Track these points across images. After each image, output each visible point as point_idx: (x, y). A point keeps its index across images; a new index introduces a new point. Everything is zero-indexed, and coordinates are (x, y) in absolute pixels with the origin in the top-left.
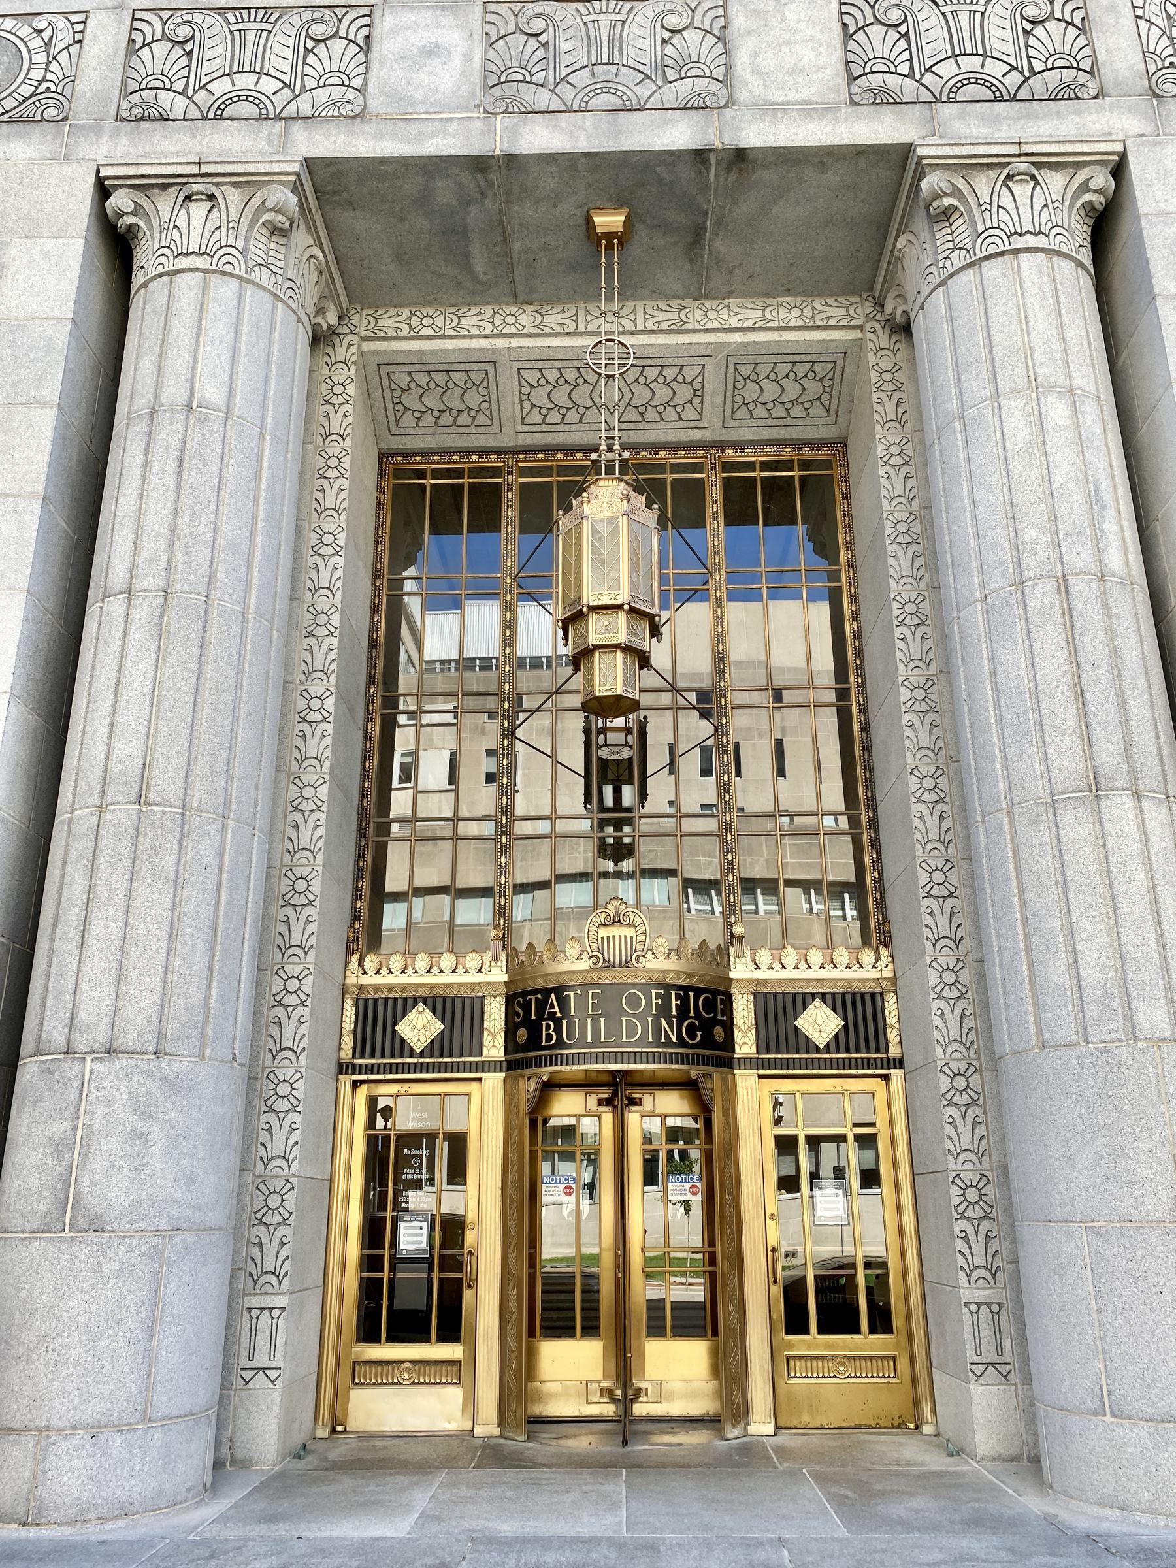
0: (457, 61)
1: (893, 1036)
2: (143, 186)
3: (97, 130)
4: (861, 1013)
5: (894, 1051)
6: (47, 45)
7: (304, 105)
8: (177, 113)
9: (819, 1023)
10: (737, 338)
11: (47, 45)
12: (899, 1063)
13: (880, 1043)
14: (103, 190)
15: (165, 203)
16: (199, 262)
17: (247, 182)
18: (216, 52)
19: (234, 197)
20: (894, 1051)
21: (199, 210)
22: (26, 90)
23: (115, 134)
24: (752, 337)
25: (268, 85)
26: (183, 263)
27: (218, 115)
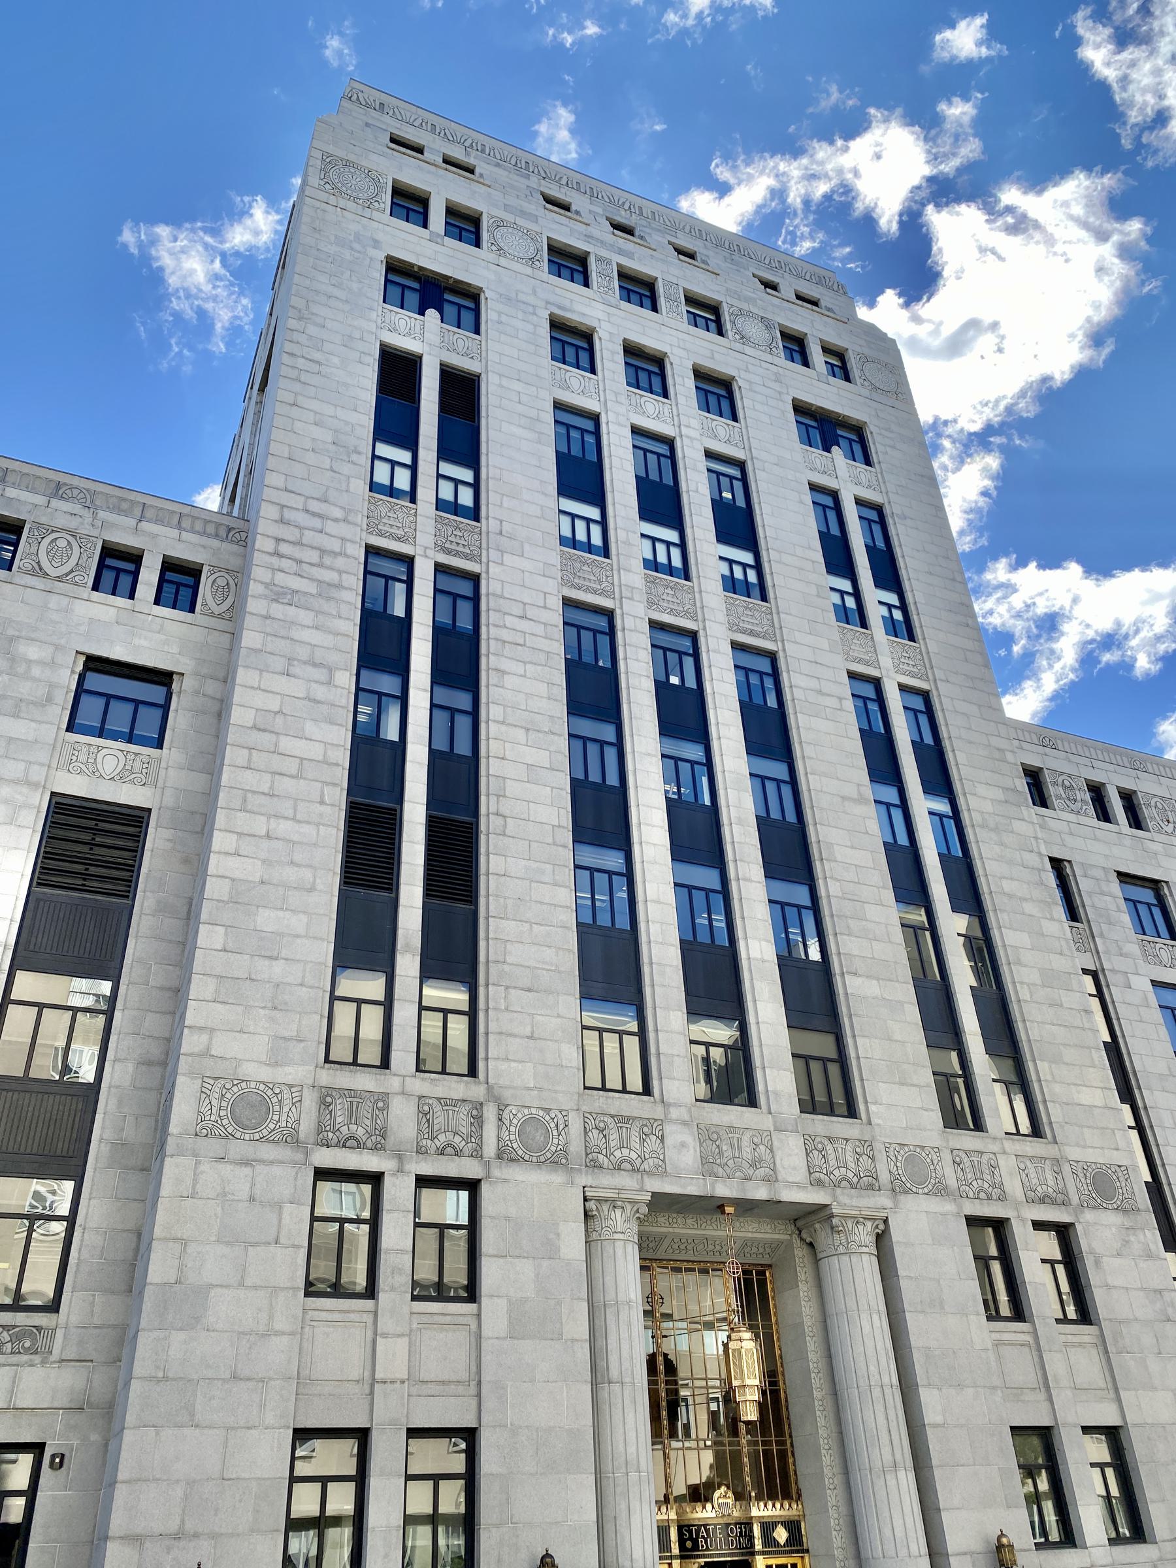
0: (692, 1151)
1: (804, 1539)
2: (599, 1200)
3: (580, 1170)
4: (793, 1527)
5: (805, 1547)
6: (557, 1125)
7: (645, 1166)
8: (605, 1166)
9: (781, 1535)
10: (750, 1235)
11: (557, 1125)
12: (807, 1551)
13: (801, 1544)
14: (585, 1200)
15: (605, 1207)
16: (621, 1236)
17: (633, 1202)
18: (614, 1136)
19: (628, 1207)
20: (805, 1547)
21: (618, 1212)
22: (553, 1149)
23: (587, 1174)
24: (755, 1235)
25: (634, 1156)
26: (616, 1236)
27: (618, 1168)
